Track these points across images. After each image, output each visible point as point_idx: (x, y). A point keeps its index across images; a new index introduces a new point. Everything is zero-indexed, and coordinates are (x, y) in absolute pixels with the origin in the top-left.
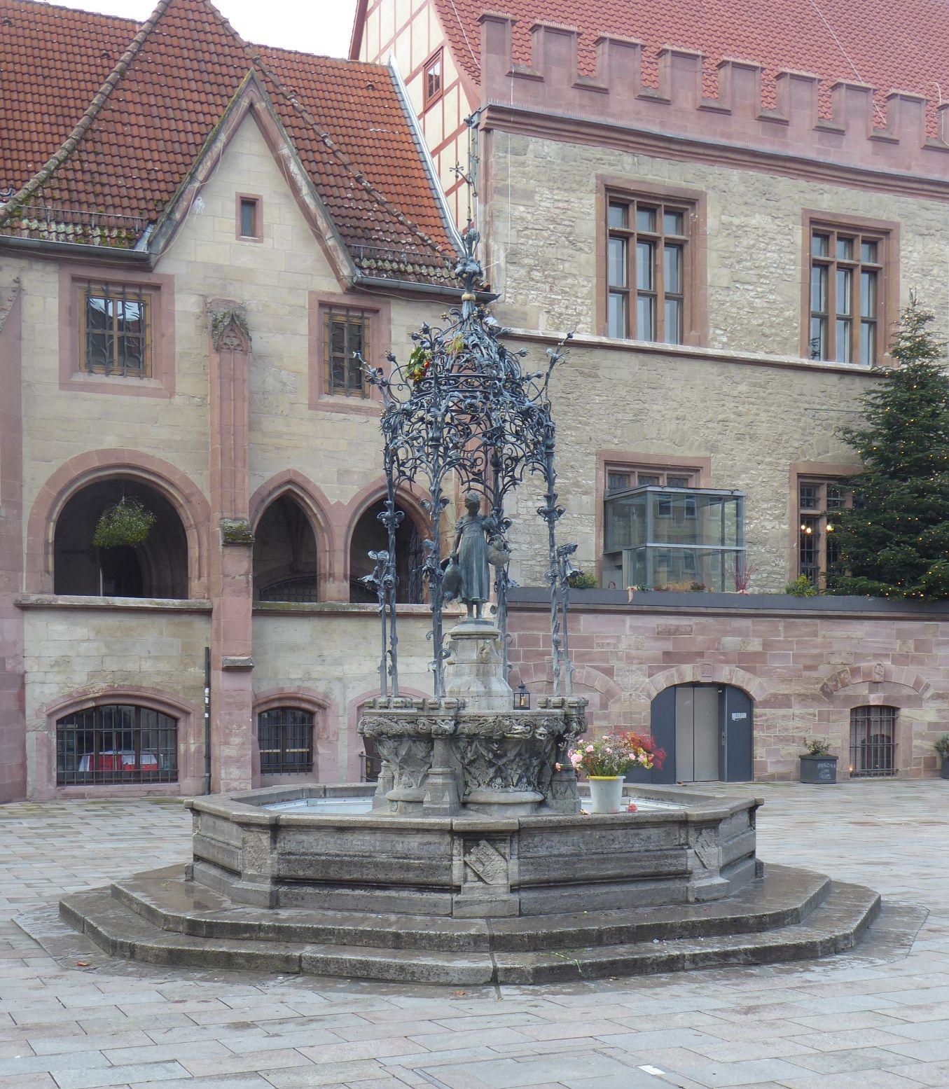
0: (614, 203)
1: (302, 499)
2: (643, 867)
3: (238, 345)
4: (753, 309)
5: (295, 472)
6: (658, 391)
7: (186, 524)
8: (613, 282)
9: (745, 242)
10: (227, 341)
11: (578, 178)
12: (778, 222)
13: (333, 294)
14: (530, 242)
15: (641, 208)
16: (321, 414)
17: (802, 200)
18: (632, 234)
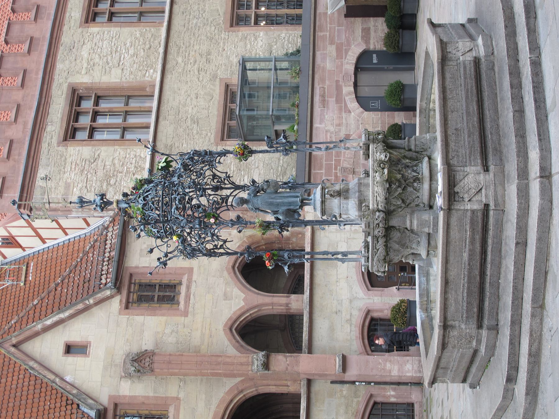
0: (73, 136)
1: (241, 322)
2: (472, 87)
3: (149, 358)
4: (136, 55)
5: (225, 326)
6: (180, 109)
7: (255, 393)
8: (118, 137)
9: (97, 60)
10: (147, 364)
11: (59, 157)
12: (86, 41)
13: (121, 301)
14: (94, 185)
15: (76, 120)
16: (190, 309)
17: (75, 28)
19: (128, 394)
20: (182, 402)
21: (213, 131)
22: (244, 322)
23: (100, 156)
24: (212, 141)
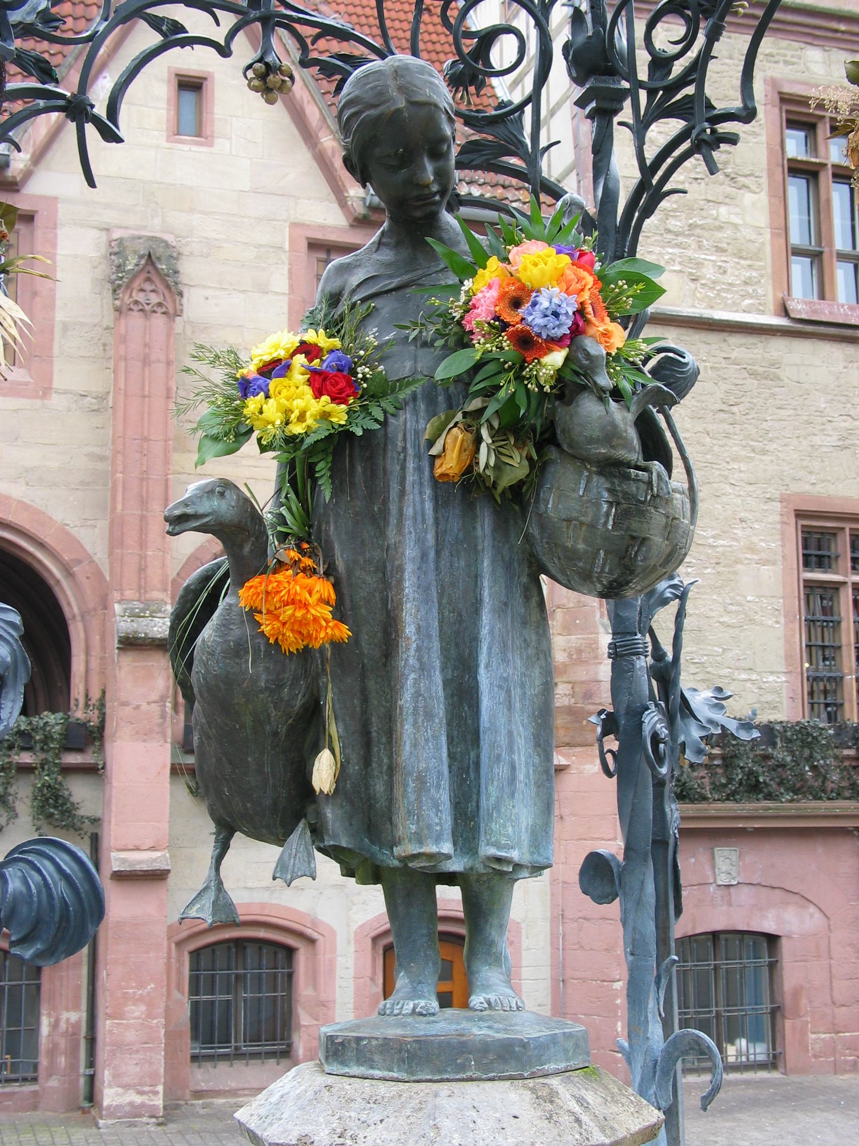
0: (793, 123)
3: (160, 305)
8: (797, 238)
10: (141, 297)
18: (823, 165)
19: (59, 251)
20: (38, 403)
21: (820, 490)
23: (741, 191)
24: (795, 488)
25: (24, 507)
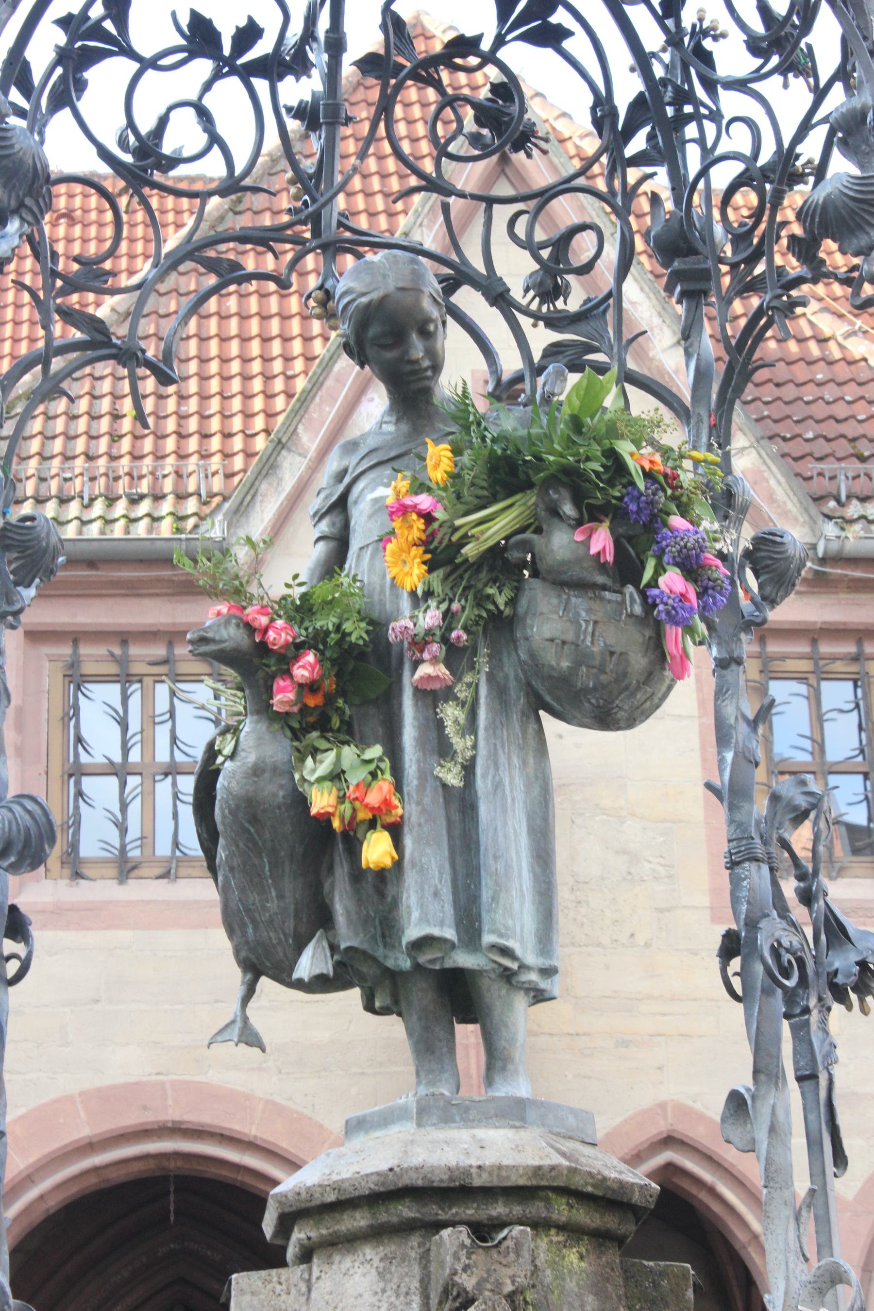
1: (712, 1191)
22: (716, 1207)
25: (275, 1109)
